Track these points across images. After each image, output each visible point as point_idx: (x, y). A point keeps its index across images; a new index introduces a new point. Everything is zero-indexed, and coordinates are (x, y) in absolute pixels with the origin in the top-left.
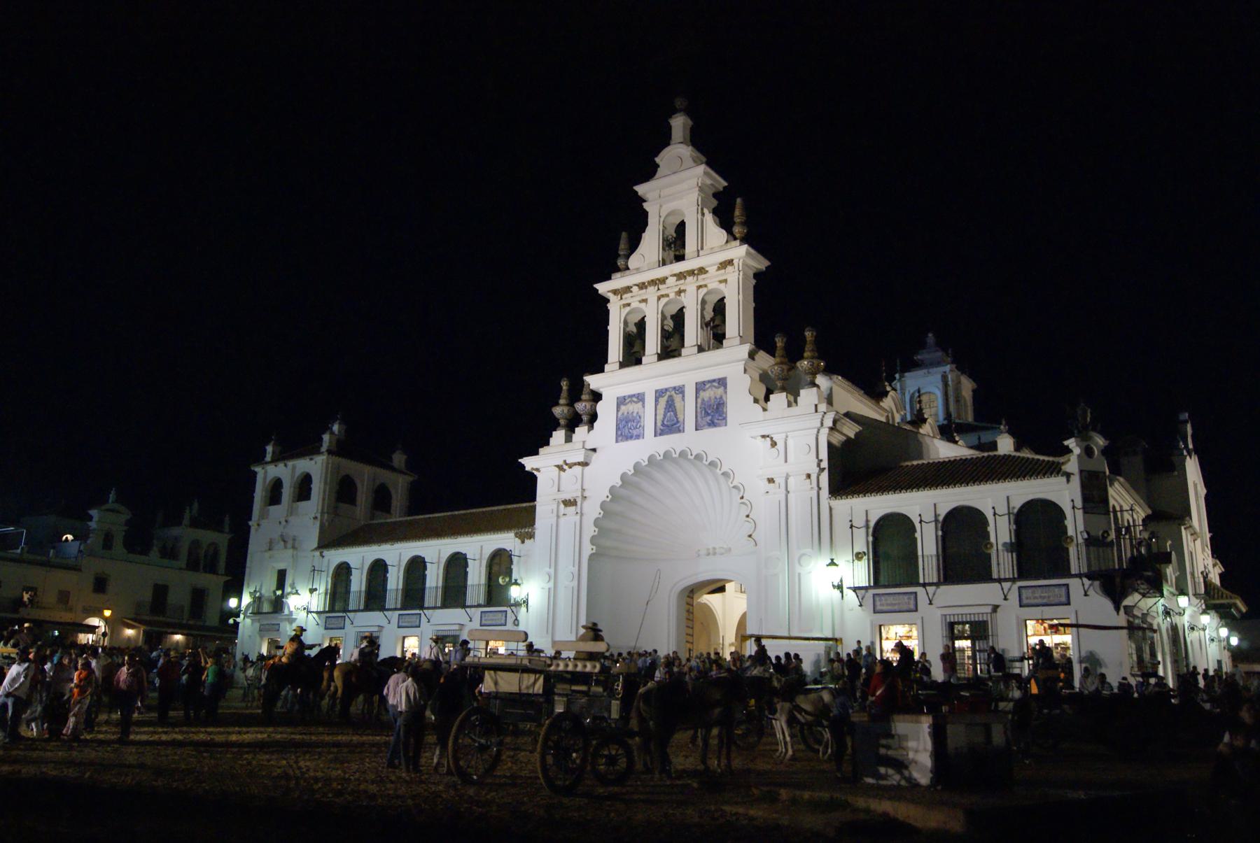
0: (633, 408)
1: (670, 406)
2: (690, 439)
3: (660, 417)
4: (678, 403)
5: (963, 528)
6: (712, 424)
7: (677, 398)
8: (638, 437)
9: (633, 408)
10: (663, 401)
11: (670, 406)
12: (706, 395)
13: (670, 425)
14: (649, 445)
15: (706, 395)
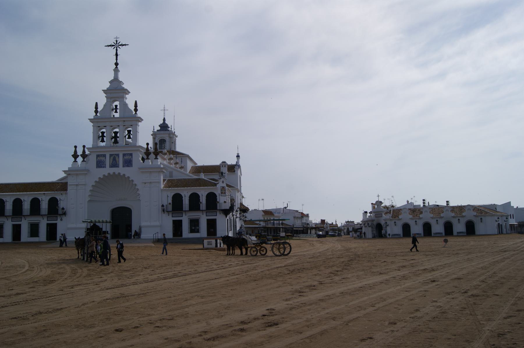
0: (102, 158)
1: (114, 159)
2: (121, 170)
3: (111, 162)
4: (117, 159)
5: (194, 198)
6: (128, 166)
7: (117, 157)
8: (104, 167)
9: (102, 158)
10: (112, 158)
11: (114, 159)
12: (126, 157)
13: (114, 165)
14: (108, 170)
15: (126, 157)
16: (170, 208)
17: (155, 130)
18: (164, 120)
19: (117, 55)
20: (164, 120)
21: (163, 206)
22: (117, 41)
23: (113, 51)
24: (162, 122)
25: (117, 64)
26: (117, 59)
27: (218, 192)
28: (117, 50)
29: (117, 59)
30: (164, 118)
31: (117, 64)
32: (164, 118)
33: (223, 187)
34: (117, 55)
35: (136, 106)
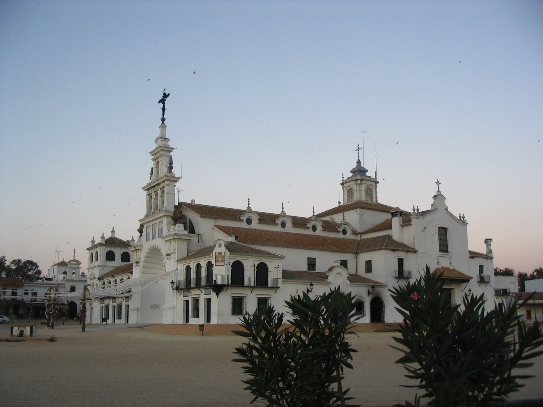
11: (155, 231)
13: (154, 238)
16: (183, 286)
17: (345, 178)
18: (359, 162)
19: (164, 109)
20: (359, 162)
21: (172, 283)
22: (164, 94)
23: (161, 105)
24: (354, 165)
25: (163, 120)
26: (163, 114)
27: (213, 262)
28: (164, 104)
29: (163, 114)
30: (359, 160)
31: (163, 120)
32: (359, 160)
33: (220, 253)
34: (164, 109)
35: (171, 164)
